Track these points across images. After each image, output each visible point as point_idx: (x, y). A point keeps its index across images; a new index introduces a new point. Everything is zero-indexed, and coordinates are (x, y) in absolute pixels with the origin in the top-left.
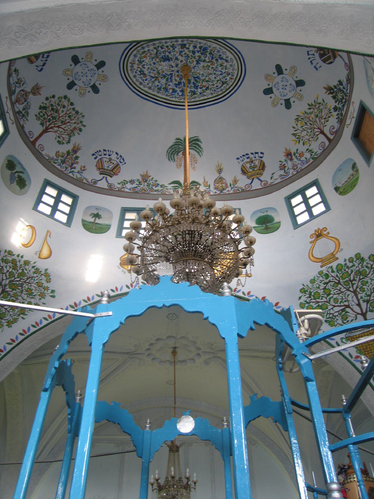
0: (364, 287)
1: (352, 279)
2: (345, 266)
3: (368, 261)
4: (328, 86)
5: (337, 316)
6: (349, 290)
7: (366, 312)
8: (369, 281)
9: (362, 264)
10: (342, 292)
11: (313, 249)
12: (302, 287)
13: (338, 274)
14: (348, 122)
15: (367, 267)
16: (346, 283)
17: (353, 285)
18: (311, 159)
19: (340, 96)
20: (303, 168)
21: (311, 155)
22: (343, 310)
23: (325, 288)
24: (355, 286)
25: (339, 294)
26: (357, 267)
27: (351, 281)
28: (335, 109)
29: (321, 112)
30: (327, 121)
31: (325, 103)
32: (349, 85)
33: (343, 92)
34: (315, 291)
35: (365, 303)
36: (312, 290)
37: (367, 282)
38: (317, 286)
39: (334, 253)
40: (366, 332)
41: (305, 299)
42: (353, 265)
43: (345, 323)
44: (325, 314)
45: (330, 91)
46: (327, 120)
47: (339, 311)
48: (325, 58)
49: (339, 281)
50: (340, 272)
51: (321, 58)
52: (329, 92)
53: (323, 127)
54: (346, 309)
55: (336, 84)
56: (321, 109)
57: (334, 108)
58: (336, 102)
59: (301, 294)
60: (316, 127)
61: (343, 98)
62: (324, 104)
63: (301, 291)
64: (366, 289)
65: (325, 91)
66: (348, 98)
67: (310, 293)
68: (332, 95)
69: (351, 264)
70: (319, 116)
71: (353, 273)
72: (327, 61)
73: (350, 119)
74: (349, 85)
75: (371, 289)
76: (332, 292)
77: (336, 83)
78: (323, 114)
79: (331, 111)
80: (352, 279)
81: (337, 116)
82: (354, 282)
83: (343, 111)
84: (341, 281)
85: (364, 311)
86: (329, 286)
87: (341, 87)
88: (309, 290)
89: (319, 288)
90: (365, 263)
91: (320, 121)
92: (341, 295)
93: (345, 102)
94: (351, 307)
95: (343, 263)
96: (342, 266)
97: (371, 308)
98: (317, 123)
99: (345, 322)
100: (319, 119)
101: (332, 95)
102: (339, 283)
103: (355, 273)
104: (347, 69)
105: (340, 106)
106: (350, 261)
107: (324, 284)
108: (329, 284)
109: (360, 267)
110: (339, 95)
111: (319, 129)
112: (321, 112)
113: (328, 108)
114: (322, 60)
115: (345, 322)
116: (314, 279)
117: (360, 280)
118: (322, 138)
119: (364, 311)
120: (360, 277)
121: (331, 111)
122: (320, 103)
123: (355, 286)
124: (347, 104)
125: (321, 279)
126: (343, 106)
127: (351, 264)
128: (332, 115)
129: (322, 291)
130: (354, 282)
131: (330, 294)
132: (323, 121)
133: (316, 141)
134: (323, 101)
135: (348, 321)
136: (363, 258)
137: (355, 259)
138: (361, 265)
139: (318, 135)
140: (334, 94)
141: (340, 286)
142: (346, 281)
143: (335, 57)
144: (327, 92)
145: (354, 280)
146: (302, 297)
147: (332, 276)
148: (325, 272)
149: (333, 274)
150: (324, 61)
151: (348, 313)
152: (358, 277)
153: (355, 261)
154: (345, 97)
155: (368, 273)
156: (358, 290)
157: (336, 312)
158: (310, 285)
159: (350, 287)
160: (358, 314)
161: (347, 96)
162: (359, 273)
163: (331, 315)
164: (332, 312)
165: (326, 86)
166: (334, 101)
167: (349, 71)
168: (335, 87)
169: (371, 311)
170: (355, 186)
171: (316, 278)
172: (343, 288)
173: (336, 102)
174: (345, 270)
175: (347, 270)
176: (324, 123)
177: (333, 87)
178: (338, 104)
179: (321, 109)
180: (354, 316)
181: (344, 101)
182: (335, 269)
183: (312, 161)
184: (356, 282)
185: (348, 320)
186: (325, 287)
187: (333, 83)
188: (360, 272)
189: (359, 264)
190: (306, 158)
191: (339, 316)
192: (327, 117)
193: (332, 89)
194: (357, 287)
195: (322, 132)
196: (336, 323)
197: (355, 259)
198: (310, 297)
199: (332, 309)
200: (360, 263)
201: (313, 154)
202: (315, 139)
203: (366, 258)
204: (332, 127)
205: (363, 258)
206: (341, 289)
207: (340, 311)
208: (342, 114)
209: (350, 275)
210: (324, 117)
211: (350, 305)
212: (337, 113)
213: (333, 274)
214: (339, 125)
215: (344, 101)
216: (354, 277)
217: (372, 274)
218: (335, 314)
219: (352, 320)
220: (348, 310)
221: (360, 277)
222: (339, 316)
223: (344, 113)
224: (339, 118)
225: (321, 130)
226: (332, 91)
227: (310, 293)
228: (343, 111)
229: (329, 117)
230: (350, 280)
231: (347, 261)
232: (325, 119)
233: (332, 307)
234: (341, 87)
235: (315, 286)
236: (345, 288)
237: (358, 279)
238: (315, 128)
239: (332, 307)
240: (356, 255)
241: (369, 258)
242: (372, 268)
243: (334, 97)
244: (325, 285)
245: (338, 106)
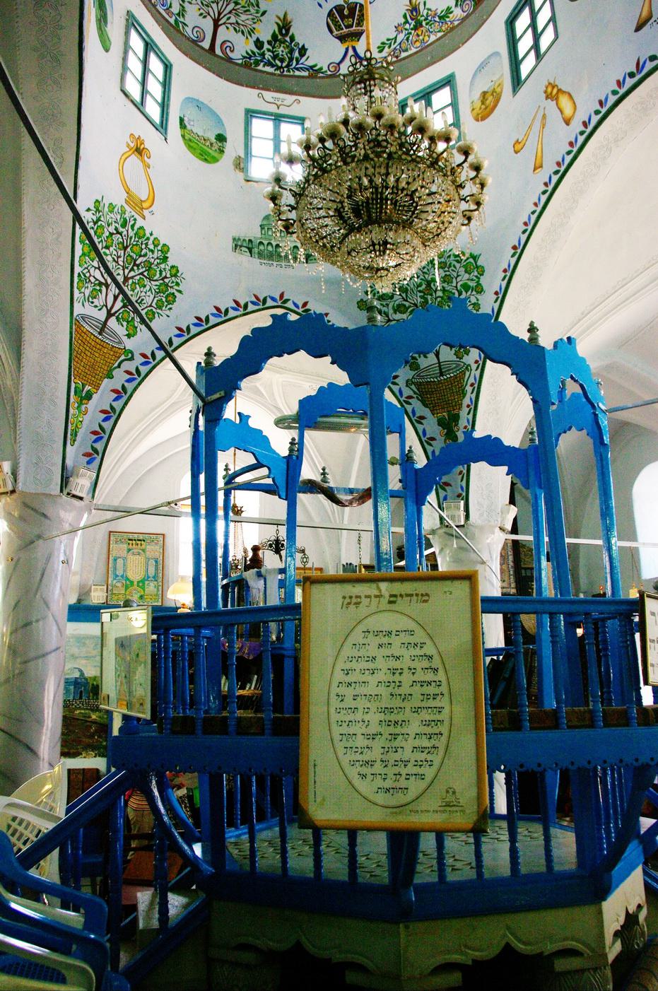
0: (137, 286)
1: (138, 262)
2: (146, 240)
3: (168, 268)
4: (290, 22)
5: (92, 283)
6: (124, 270)
7: (114, 314)
8: (148, 288)
9: (160, 264)
10: (117, 262)
11: (128, 157)
12: (100, 199)
13: (133, 238)
14: (268, 95)
15: (161, 271)
16: (129, 258)
17: (132, 269)
18: (174, 18)
19: (281, 50)
20: (158, 7)
21: (179, 14)
22: (100, 284)
23: (111, 234)
24: (132, 274)
25: (114, 260)
26: (153, 258)
27: (135, 265)
28: (259, 44)
29: (245, 11)
30: (235, 29)
31: (261, 18)
32: (306, 74)
33: (291, 60)
34: (103, 224)
35: (122, 304)
36: (102, 219)
37: (145, 286)
38: (110, 221)
39: (145, 205)
40: (94, 335)
41: (90, 220)
42: (152, 252)
43: (89, 301)
44: (86, 266)
45: (284, 27)
46: (238, 29)
47: (97, 280)
48: (336, 18)
49: (127, 247)
50: (137, 239)
51: (335, 7)
52: (281, 25)
53: (224, 23)
54: (103, 286)
55: (297, 39)
56: (248, 11)
57: (258, 39)
58: (269, 43)
59: (92, 208)
60: (220, 5)
61: (282, 61)
62: (259, 15)
63: (97, 201)
64: (136, 291)
65: (282, 17)
66: (285, 73)
67: (99, 220)
68: (277, 32)
69: (151, 247)
70: (238, 6)
71: (144, 259)
72: (332, 20)
73: (272, 100)
74: (306, 74)
75: (140, 297)
76: (111, 249)
77: (300, 40)
78: (243, 17)
79: (252, 34)
80: (138, 262)
81: (250, 53)
82: (135, 268)
83: (262, 64)
84: (129, 249)
85: (113, 311)
86: (117, 238)
87: (296, 54)
88: (101, 213)
89: (109, 226)
90: (163, 266)
91: (230, 12)
92: (114, 263)
93: (278, 68)
94: (109, 290)
95: (148, 235)
96: (145, 235)
97: (120, 317)
98: (227, 5)
99: (90, 300)
100: (233, 9)
101: (277, 32)
102: (125, 248)
103: (146, 261)
104: (331, 69)
105: (268, 55)
106: (155, 243)
107: (116, 229)
108: (119, 236)
109: (156, 263)
110: (282, 48)
111: (220, 14)
112: (245, 11)
113: (253, 26)
114: (331, 10)
115: (90, 300)
116: (114, 208)
117: (142, 274)
118: (208, 25)
119: (113, 311)
120: (145, 271)
121: (252, 34)
122: (258, 6)
123: (132, 274)
124: (276, 72)
125: (119, 217)
126: (269, 64)
127: (151, 247)
128: (247, 38)
129: (107, 234)
130: (135, 268)
131: (107, 247)
132: (233, 20)
133: (201, 14)
134: (264, 13)
135: (92, 303)
136: (167, 257)
137: (159, 248)
138: (159, 261)
139: (209, 14)
140: (280, 37)
141: (123, 252)
142: (131, 256)
143: (342, 39)
144: (280, 19)
145: (138, 266)
146: (91, 212)
147: (127, 231)
148: (127, 216)
149: (130, 230)
150: (330, 14)
151: (101, 293)
152: (144, 269)
153: (158, 251)
154: (284, 65)
155: (155, 278)
156: (130, 281)
157: (94, 277)
158: (106, 209)
159: (127, 268)
160: (106, 306)
161: (289, 71)
162: (149, 266)
163: (88, 275)
164: (92, 270)
165: (289, 18)
166: (270, 38)
167: (329, 73)
168: (292, 39)
169: (118, 319)
170: (206, 160)
171: (116, 209)
172: (122, 259)
173: (269, 43)
174: (142, 244)
175: (144, 246)
176: (231, 24)
177: (290, 33)
178: (269, 50)
179: (248, 11)
180: (102, 304)
181: (279, 64)
182: (136, 228)
183: (172, 21)
184: (137, 273)
185: (94, 300)
186: (113, 234)
187: (301, 34)
188: (150, 267)
189: (157, 258)
190: (170, 6)
191: (93, 285)
192: (242, 27)
193: (288, 31)
194: (132, 278)
195: (216, 26)
196: (83, 290)
197: (159, 248)
198: (95, 223)
199: (96, 268)
200: (160, 259)
201: (182, 19)
202: (202, 11)
203: (171, 262)
204: (231, 46)
205: (167, 257)
206: (120, 257)
207: (97, 282)
208: (257, 64)
209: (140, 256)
210: (240, 22)
211: (110, 287)
212: (256, 50)
213: (130, 230)
214: (240, 62)
215: (279, 64)
216: (141, 263)
217: (156, 285)
218: (92, 279)
219: (96, 306)
220: (104, 289)
221: (145, 271)
222: (93, 285)
223: (260, 67)
224: (250, 58)
225: (219, 20)
226: (284, 32)
227: (99, 220)
228: (264, 66)
229: (243, 33)
230: (135, 260)
231: (152, 239)
232: (237, 23)
233: (97, 266)
234: (296, 54)
235: (108, 216)
236: (123, 262)
237: (140, 271)
238: (217, 4)
239: (97, 266)
240: (164, 245)
241: (173, 267)
242: (163, 279)
243: (274, 36)
244: (115, 232)
245: (265, 49)
